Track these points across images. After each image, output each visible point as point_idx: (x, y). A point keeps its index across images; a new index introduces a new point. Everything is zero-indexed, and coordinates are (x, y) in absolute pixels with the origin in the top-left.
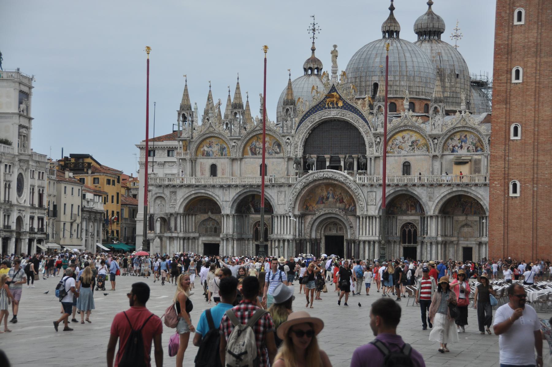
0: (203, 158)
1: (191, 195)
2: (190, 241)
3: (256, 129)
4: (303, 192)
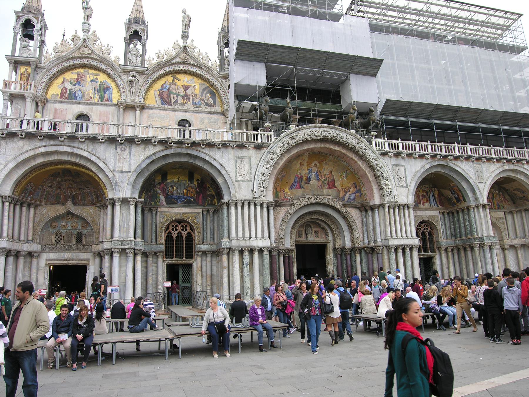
0: (61, 102)
1: (34, 157)
2: (21, 260)
3: (174, 61)
4: (281, 163)
